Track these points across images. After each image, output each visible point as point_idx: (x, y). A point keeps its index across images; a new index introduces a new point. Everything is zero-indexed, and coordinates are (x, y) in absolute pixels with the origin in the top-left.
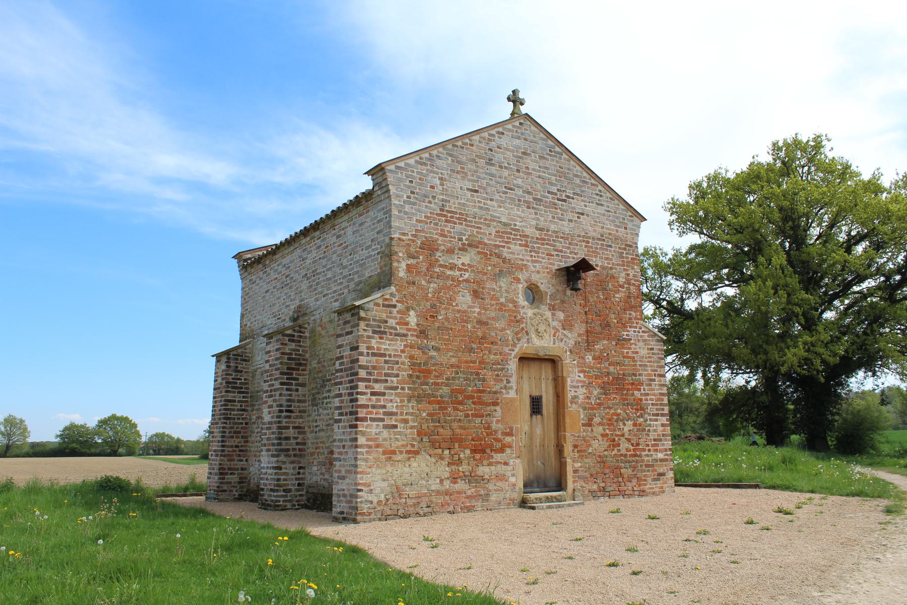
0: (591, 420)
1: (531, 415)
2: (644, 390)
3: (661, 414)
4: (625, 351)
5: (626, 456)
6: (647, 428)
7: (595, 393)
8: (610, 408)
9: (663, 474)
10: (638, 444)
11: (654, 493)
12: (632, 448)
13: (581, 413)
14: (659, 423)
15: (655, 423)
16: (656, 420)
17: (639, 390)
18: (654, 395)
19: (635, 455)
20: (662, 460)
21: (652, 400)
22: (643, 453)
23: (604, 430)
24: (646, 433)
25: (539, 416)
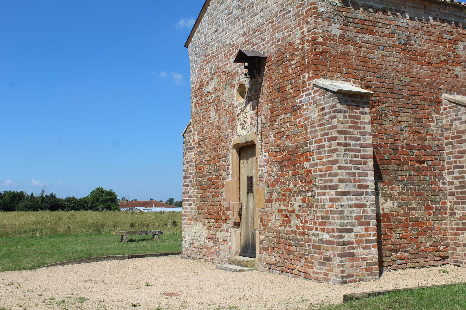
0: (271, 196)
1: (248, 194)
2: (314, 160)
3: (330, 186)
4: (298, 120)
5: (295, 232)
6: (315, 204)
7: (275, 169)
8: (284, 183)
9: (328, 259)
10: (306, 222)
11: (317, 279)
12: (301, 225)
13: (265, 189)
14: (327, 197)
15: (323, 197)
16: (324, 194)
17: (309, 160)
18: (323, 164)
19: (304, 234)
20: (329, 243)
21: (320, 170)
22: (311, 232)
23: (280, 205)
24: (314, 209)
25: (252, 194)
